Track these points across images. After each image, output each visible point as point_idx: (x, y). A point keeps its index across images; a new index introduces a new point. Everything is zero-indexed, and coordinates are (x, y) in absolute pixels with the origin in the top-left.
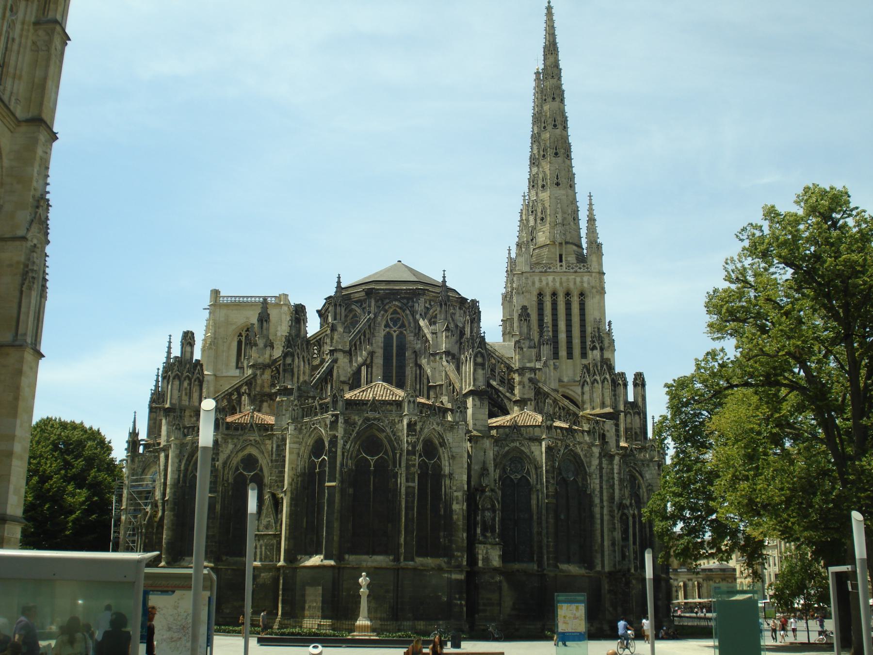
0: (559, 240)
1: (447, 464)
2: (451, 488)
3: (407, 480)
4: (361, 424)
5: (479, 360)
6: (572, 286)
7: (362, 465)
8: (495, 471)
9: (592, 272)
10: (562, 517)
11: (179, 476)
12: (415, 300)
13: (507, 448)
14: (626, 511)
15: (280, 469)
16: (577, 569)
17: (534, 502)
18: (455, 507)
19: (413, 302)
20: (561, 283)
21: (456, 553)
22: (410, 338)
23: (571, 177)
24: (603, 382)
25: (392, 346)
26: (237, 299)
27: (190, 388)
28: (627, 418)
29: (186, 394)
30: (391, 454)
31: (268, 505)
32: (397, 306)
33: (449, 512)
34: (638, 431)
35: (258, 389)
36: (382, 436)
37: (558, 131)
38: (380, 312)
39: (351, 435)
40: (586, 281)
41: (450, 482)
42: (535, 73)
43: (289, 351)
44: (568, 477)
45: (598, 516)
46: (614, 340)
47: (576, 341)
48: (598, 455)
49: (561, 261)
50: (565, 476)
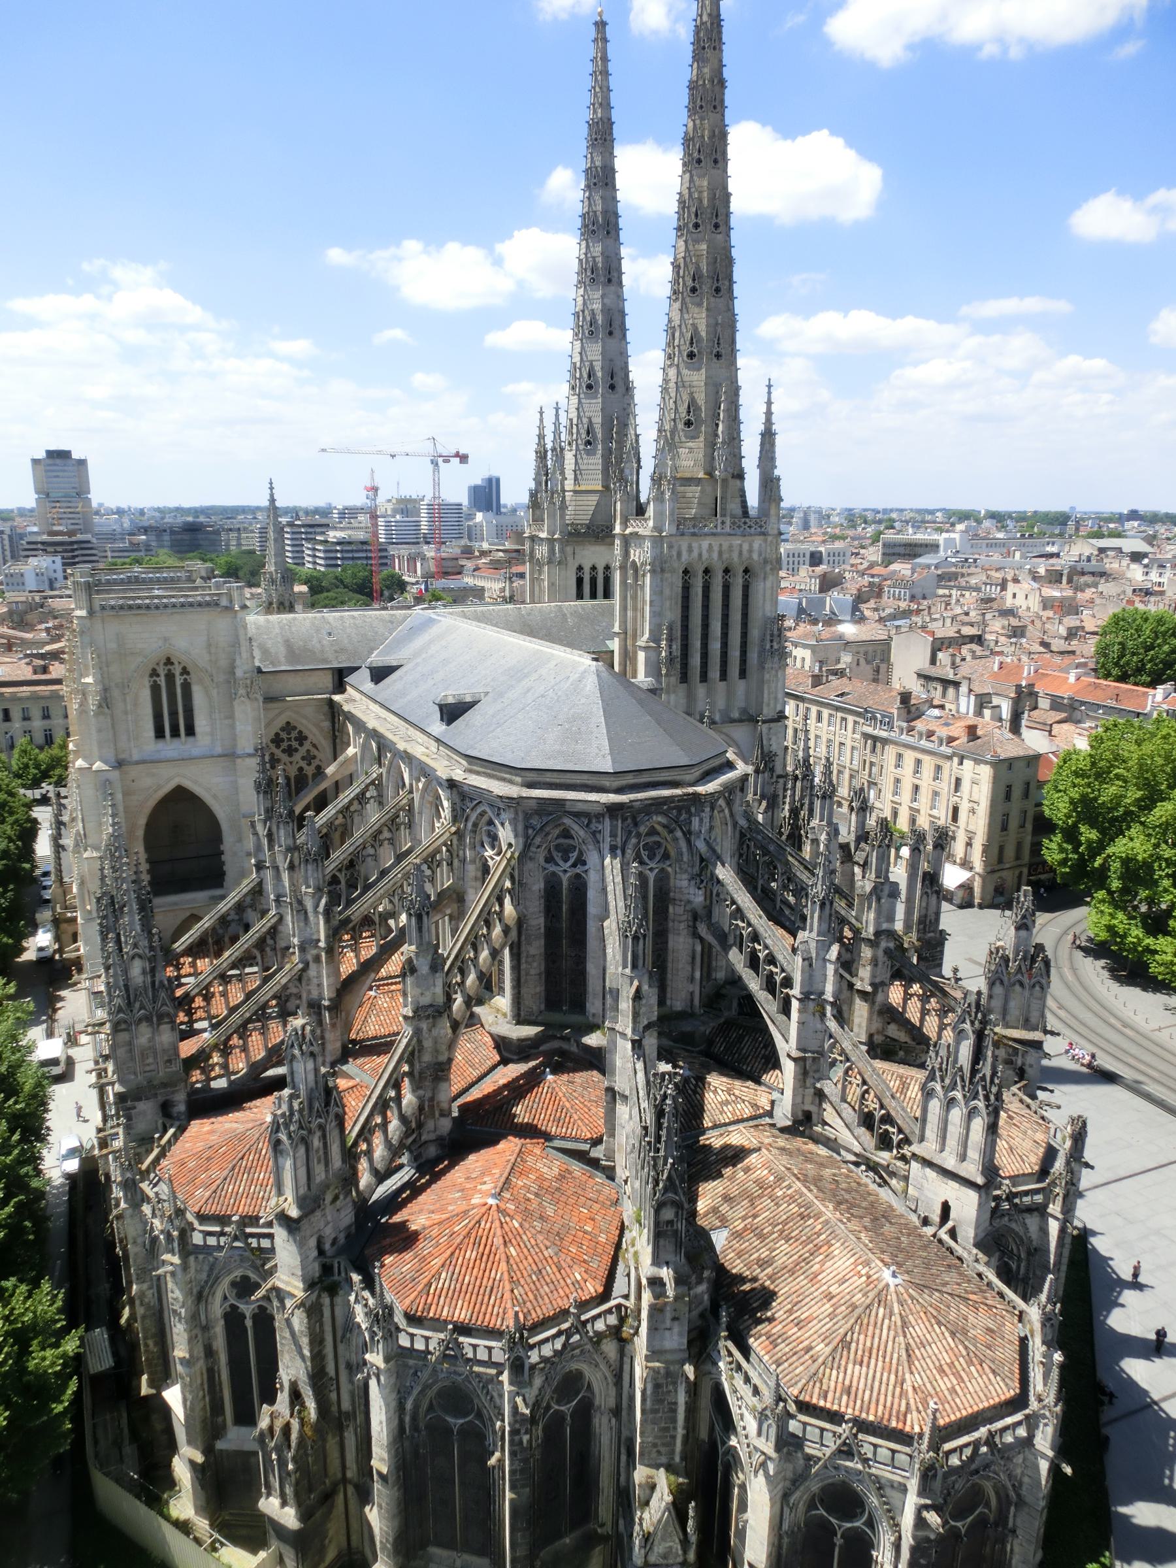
12: (693, 810)
15: (663, 1425)
19: (690, 815)
20: (720, 553)
29: (319, 1162)
32: (659, 823)
42: (596, 24)
47: (735, 654)
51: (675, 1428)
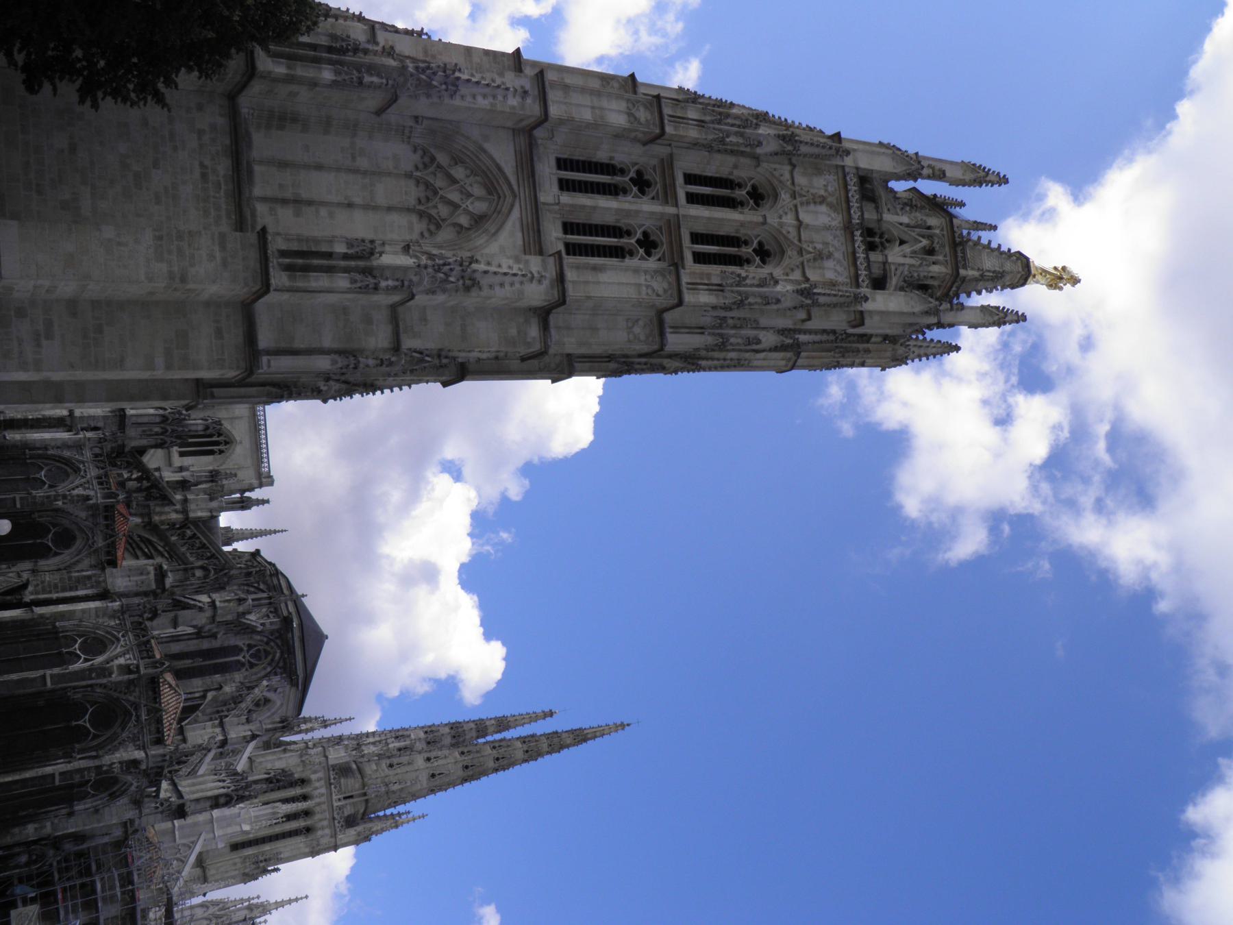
1: (87, 806)
2: (56, 817)
4: (130, 701)
5: (222, 800)
6: (317, 817)
9: (336, 838)
11: (39, 449)
12: (284, 675)
19: (281, 674)
23: (443, 788)
25: (225, 657)
26: (263, 427)
27: (153, 435)
30: (95, 743)
31: (11, 582)
32: (274, 657)
33: (23, 822)
35: (158, 509)
37: (491, 764)
39: (115, 691)
40: (323, 834)
42: (551, 711)
43: (209, 571)
46: (257, 879)
51: (57, 592)
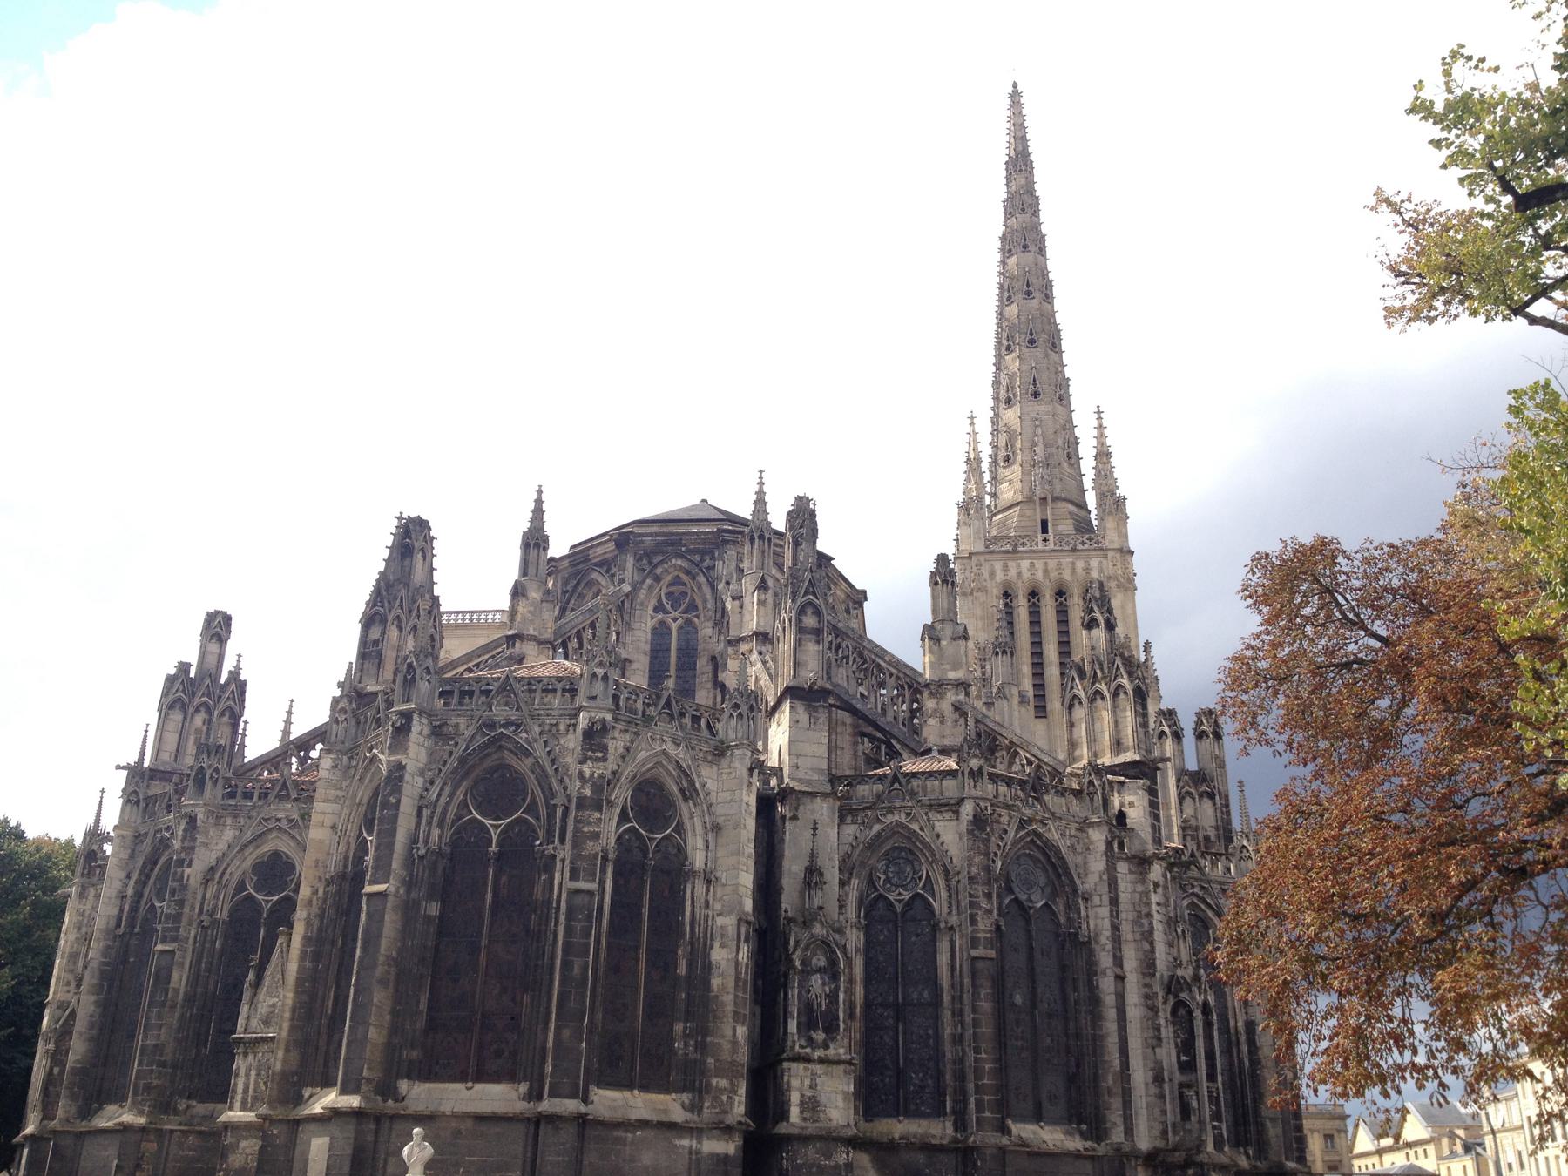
0: (1039, 494)
1: (700, 844)
2: (707, 905)
3: (574, 875)
4: (473, 736)
5: (810, 621)
6: (1067, 576)
7: (465, 844)
8: (843, 883)
9: (1107, 550)
10: (1018, 999)
11: (121, 910)
13: (877, 828)
14: (1184, 995)
16: (1062, 1137)
17: (943, 959)
18: (719, 955)
19: (713, 558)
20: (1046, 572)
21: (714, 1081)
22: (706, 630)
24: (1115, 695)
25: (669, 650)
27: (208, 729)
28: (1185, 805)
30: (543, 811)
33: (702, 967)
34: (1212, 833)
36: (524, 766)
37: (1034, 303)
38: (644, 581)
39: (444, 764)
40: (1097, 567)
41: (708, 891)
44: (1030, 900)
45: (1109, 1000)
48: (1102, 847)
49: (1045, 530)
50: (1023, 897)
